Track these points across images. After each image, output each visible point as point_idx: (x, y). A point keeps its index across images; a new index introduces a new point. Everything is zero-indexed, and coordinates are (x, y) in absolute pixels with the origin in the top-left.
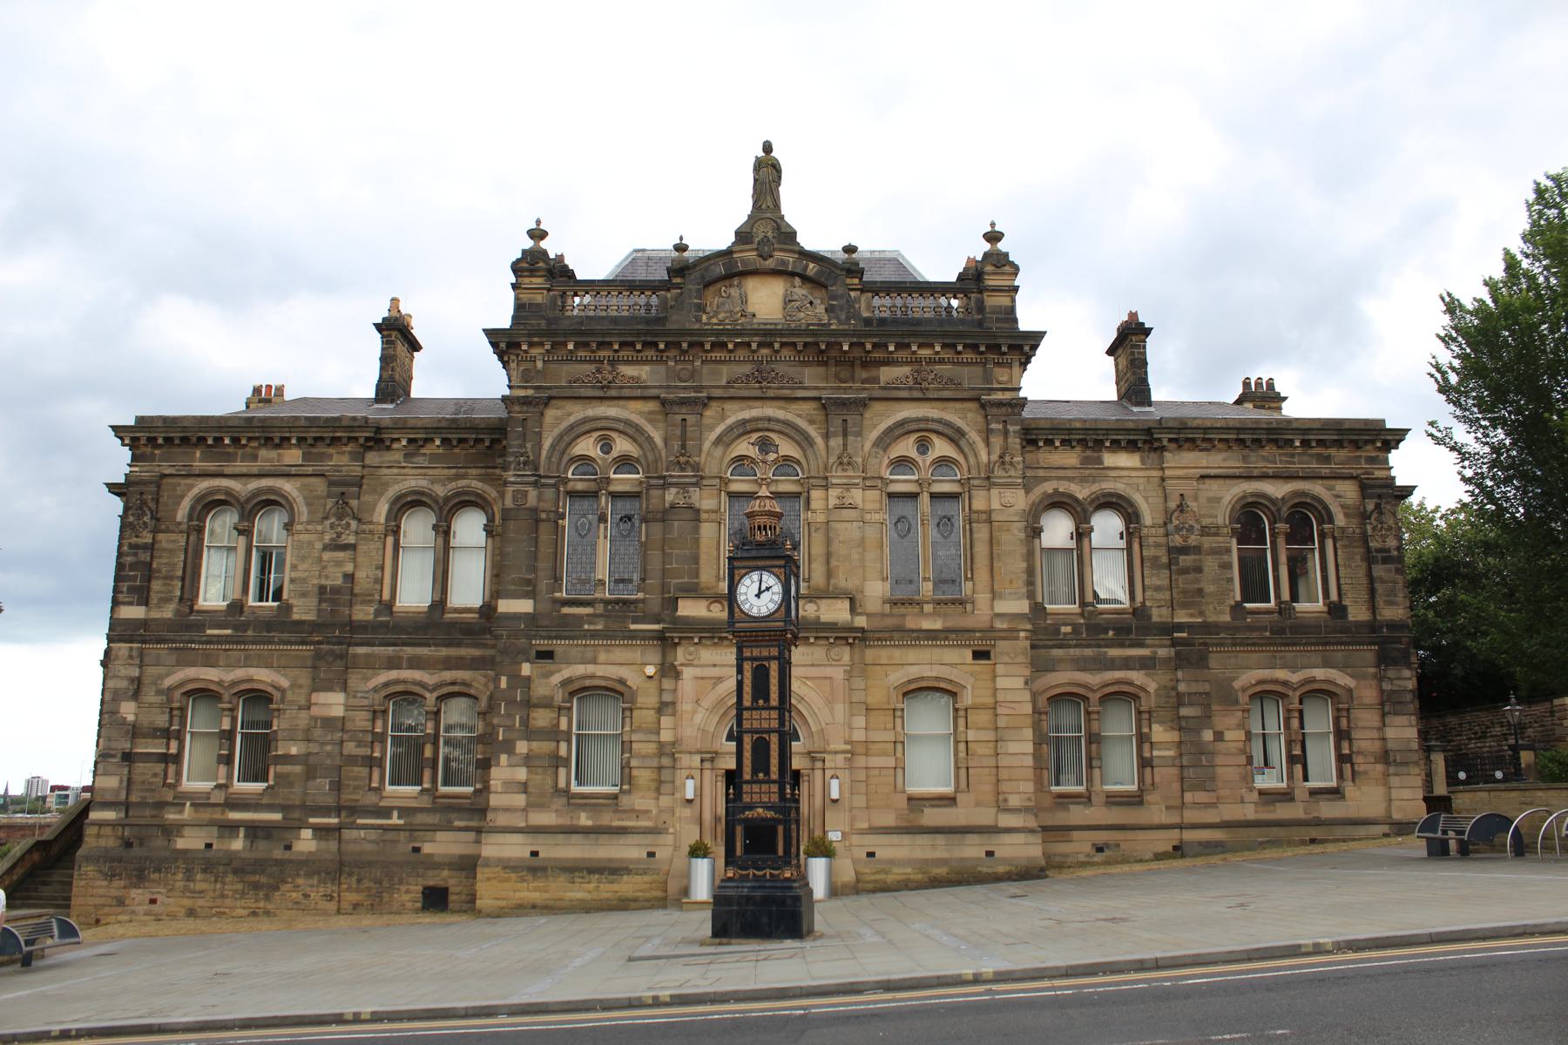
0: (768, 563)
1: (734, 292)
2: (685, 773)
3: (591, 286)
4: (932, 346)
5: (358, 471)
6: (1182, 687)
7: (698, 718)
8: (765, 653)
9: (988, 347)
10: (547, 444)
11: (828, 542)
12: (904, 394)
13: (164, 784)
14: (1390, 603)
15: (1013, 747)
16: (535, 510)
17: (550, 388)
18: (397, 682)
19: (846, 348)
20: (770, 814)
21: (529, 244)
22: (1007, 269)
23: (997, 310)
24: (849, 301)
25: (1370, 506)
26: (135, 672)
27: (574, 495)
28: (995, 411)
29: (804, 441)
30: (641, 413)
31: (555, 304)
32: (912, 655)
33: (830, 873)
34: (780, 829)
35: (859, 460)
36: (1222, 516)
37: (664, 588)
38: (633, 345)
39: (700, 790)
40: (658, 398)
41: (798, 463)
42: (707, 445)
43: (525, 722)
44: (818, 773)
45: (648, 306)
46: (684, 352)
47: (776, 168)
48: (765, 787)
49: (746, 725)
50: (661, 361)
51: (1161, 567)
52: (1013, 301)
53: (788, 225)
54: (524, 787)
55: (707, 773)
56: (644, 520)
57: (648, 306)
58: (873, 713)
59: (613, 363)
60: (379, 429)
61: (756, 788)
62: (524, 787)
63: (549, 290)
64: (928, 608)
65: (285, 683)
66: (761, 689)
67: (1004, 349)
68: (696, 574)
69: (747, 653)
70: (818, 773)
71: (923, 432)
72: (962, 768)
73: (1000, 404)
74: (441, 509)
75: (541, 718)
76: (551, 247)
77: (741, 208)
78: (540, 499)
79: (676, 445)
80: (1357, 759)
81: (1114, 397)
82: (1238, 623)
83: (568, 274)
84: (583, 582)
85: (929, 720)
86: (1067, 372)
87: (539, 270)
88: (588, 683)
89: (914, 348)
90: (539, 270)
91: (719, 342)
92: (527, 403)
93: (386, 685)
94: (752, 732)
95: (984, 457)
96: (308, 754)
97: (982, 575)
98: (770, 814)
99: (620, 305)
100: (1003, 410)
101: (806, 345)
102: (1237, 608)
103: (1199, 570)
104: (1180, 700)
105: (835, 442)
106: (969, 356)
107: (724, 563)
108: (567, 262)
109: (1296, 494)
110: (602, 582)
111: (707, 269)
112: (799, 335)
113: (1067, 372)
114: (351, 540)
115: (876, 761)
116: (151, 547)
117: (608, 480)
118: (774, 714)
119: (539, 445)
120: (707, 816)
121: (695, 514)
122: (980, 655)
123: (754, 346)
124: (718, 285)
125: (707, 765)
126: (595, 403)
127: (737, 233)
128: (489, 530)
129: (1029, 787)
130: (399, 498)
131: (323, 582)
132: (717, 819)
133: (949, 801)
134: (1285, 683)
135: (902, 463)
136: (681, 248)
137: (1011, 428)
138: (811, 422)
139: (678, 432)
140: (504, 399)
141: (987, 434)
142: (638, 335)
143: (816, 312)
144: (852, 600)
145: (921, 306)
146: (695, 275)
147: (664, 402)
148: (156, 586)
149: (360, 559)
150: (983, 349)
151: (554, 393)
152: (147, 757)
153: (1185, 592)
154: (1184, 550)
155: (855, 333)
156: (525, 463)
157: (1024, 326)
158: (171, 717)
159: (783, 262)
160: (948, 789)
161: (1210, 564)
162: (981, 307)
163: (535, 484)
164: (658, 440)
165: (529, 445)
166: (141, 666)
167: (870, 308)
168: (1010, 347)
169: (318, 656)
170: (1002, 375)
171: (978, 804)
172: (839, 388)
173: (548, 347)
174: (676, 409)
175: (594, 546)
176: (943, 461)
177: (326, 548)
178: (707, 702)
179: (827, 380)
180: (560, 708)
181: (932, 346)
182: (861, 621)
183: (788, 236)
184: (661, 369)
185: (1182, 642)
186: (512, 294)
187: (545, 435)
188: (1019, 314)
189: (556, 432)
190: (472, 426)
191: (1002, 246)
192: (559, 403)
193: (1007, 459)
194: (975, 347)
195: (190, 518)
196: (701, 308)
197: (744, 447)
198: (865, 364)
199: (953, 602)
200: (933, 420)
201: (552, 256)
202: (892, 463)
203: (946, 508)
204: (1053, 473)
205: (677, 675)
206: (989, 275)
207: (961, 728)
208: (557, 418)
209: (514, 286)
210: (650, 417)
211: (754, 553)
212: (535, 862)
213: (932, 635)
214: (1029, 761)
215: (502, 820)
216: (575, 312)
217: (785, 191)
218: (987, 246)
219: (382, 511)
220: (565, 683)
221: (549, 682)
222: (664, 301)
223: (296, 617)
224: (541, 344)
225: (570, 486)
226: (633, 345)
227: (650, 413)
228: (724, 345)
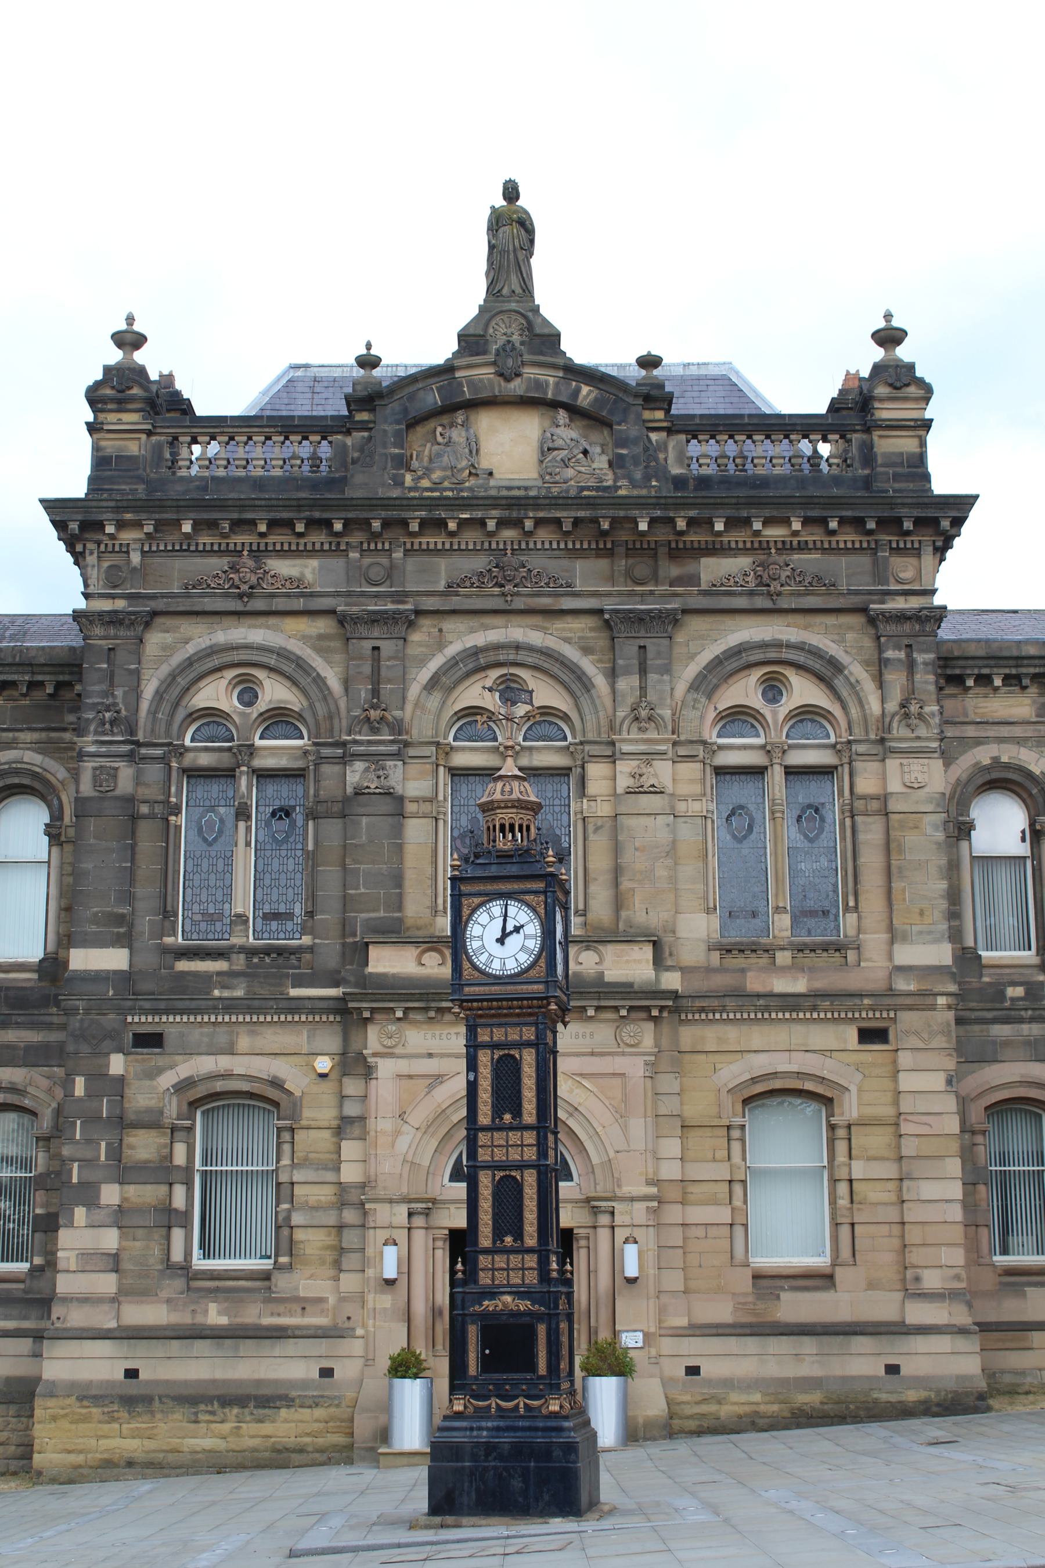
0: (516, 886)
1: (457, 435)
2: (382, 1235)
3: (219, 427)
4: (787, 522)
7: (403, 1144)
8: (514, 1035)
9: (881, 522)
10: (149, 690)
11: (617, 849)
12: (742, 602)
15: (929, 1190)
16: (130, 800)
17: (153, 597)
19: (643, 526)
20: (524, 1305)
21: (115, 356)
22: (912, 390)
23: (897, 460)
27: (194, 774)
28: (891, 629)
29: (575, 681)
30: (305, 638)
31: (160, 457)
32: (757, 1036)
33: (626, 1402)
34: (542, 1329)
35: (667, 713)
37: (345, 927)
38: (290, 524)
39: (407, 1264)
40: (332, 612)
41: (566, 718)
42: (414, 691)
43: (116, 1153)
44: (604, 1234)
45: (315, 460)
46: (375, 536)
47: (525, 225)
48: (515, 1260)
49: (483, 1155)
50: (337, 551)
52: (923, 444)
53: (546, 323)
54: (114, 1262)
55: (419, 1236)
56: (312, 815)
57: (315, 460)
58: (693, 1134)
59: (258, 554)
61: (500, 1261)
62: (114, 1262)
63: (149, 433)
64: (783, 958)
66: (507, 1096)
67: (908, 525)
68: (400, 907)
69: (484, 1036)
70: (604, 1234)
71: (773, 666)
72: (844, 1225)
73: (901, 617)
75: (143, 1146)
76: (152, 360)
77: (466, 294)
78: (138, 781)
79: (363, 691)
83: (181, 406)
84: (211, 918)
85: (786, 1144)
87: (132, 399)
88: (219, 1086)
89: (757, 525)
90: (132, 399)
91: (436, 518)
92: (115, 623)
95: (874, 706)
97: (873, 901)
98: (524, 1305)
99: (268, 458)
100: (907, 627)
101: (577, 522)
105: (628, 684)
106: (849, 537)
107: (444, 888)
108: (178, 386)
110: (242, 919)
111: (411, 397)
112: (565, 506)
115: (698, 1214)
117: (251, 750)
118: (530, 1138)
120: (420, 1308)
121: (396, 806)
122: (870, 1035)
123: (491, 525)
124: (431, 424)
125: (419, 1221)
126: (227, 621)
127: (462, 337)
128: (54, 834)
129: (957, 1257)
132: (435, 1312)
133: (822, 1280)
135: (738, 717)
136: (369, 362)
137: (920, 658)
138: (587, 650)
139: (367, 669)
140: (77, 615)
141: (879, 667)
142: (299, 508)
143: (594, 467)
144: (656, 945)
145: (767, 456)
146: (393, 407)
147: (342, 620)
150: (871, 525)
151: (160, 605)
155: (658, 502)
156: (113, 722)
157: (942, 485)
159: (539, 385)
160: (821, 1261)
162: (868, 456)
163: (131, 757)
164: (334, 683)
165: (119, 692)
167: (683, 459)
168: (918, 522)
170: (904, 568)
171: (872, 1285)
172: (631, 594)
173: (149, 529)
174: (362, 630)
175: (228, 860)
176: (806, 715)
178: (418, 1116)
179: (612, 579)
180: (173, 1129)
181: (787, 522)
182: (672, 981)
183: (547, 341)
184: (337, 564)
186: (86, 442)
187: (146, 674)
188: (934, 465)
189: (165, 670)
190: (25, 662)
191: (904, 352)
193: (914, 708)
194: (858, 523)
196: (403, 463)
197: (476, 693)
198: (678, 553)
199: (825, 948)
200: (789, 646)
201: (154, 376)
202: (721, 717)
203: (812, 791)
204: (992, 732)
205: (368, 1072)
206: (882, 402)
207: (841, 1157)
208: (165, 648)
209: (92, 428)
210: (319, 643)
211: (494, 871)
212: (132, 1388)
213: (790, 1003)
214: (956, 1213)
215: (77, 1317)
216: (194, 470)
217: (540, 264)
218: (878, 354)
220: (182, 1087)
222: (341, 452)
224: (138, 525)
225: (188, 760)
226: (290, 524)
227: (321, 637)
228: (442, 523)
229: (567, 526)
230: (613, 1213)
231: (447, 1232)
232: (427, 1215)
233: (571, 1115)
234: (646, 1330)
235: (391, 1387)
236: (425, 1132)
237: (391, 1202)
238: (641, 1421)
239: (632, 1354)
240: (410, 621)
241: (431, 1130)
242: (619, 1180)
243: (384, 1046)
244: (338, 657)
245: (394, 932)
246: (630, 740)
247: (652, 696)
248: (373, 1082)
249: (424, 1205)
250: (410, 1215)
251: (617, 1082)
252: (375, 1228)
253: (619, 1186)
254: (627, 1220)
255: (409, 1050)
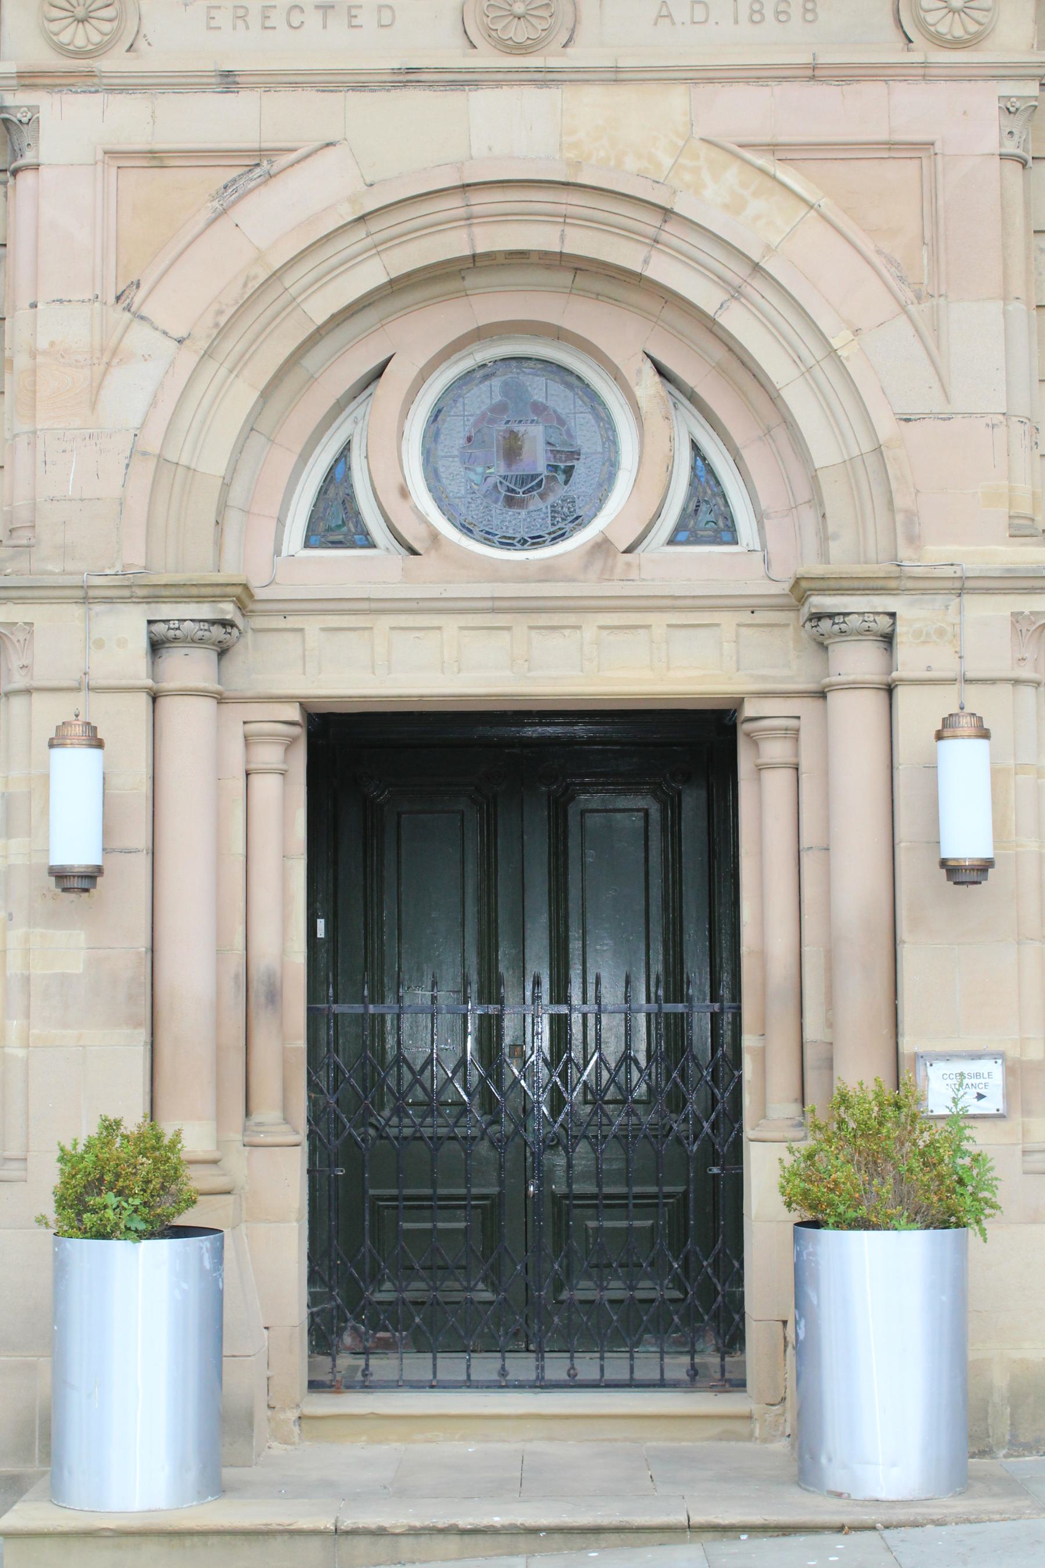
2: (48, 712)
7: (132, 395)
39: (143, 819)
44: (855, 715)
55: (189, 721)
58: (883, 695)
70: (855, 715)
120: (193, 976)
125: (190, 668)
132: (254, 993)
178: (187, 297)
230: (888, 639)
231: (294, 713)
232: (223, 652)
233: (736, 293)
234: (1013, 1053)
235: (60, 1268)
236: (208, 354)
237: (86, 600)
238: (1000, 1380)
239: (981, 1139)
241: (233, 346)
242: (911, 516)
243: (62, 50)
248: (26, 179)
249: (205, 611)
250: (156, 646)
251: (903, 173)
252: (28, 691)
253: (913, 539)
254: (945, 664)
255: (153, 60)
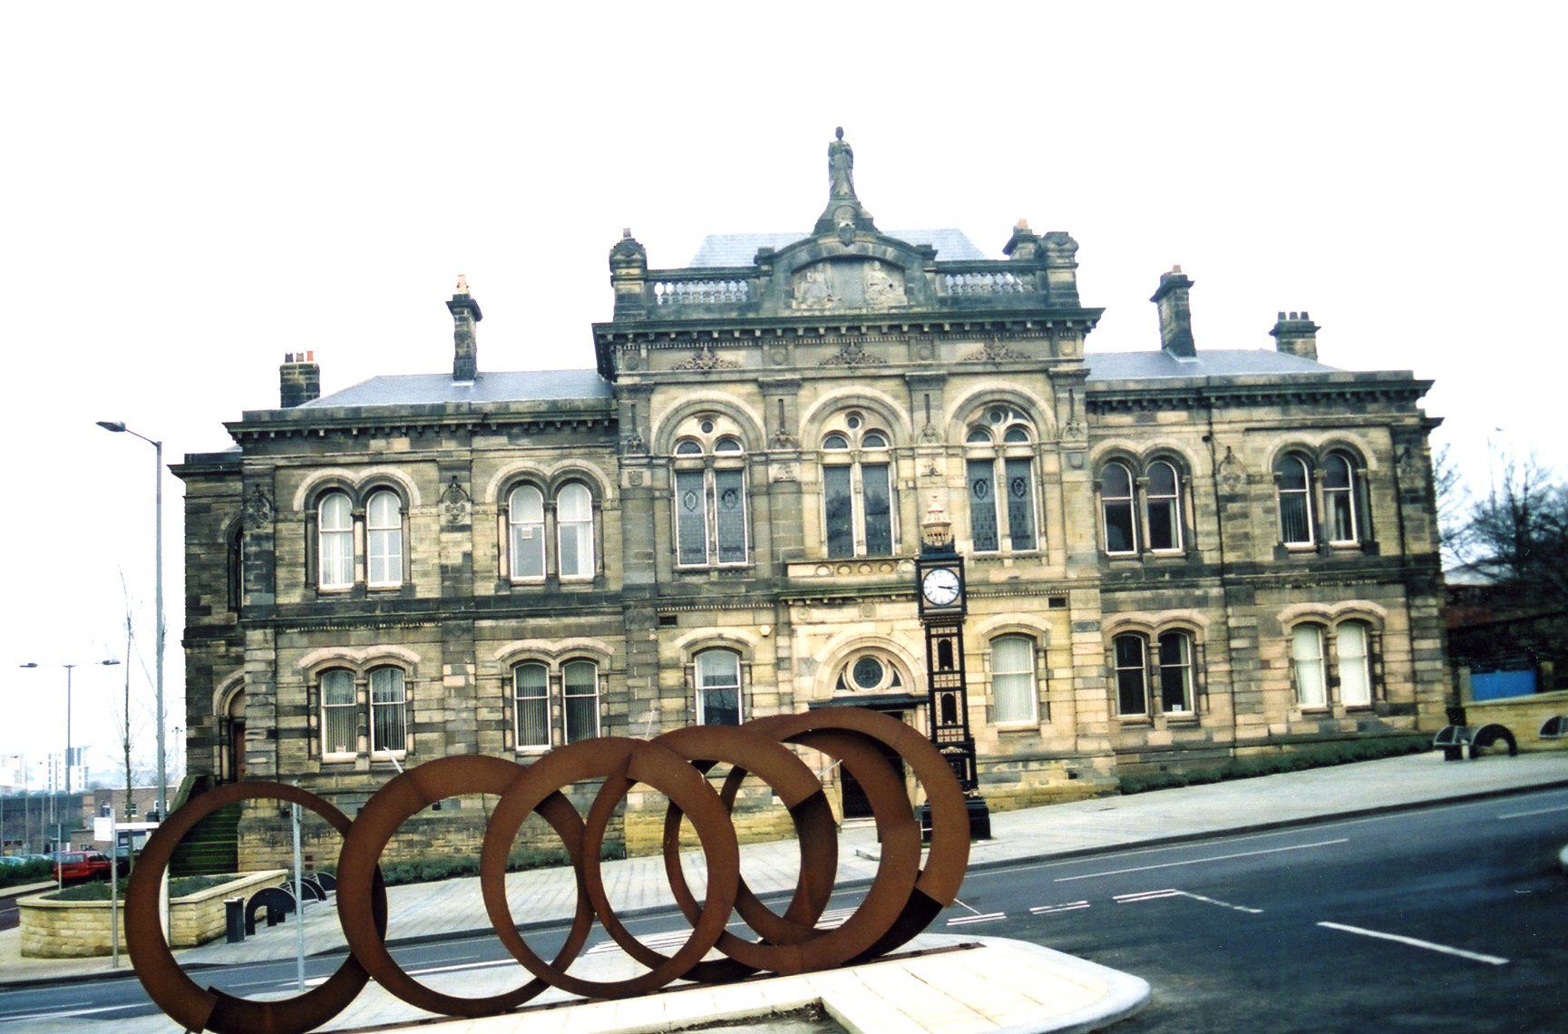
5: (467, 456)
6: (1232, 622)
8: (947, 631)
10: (655, 426)
13: (310, 757)
14: (1417, 539)
16: (650, 489)
18: (523, 651)
20: (959, 751)
24: (926, 283)
25: (1400, 450)
26: (272, 655)
27: (681, 473)
28: (1062, 382)
30: (740, 395)
36: (1265, 465)
37: (773, 555)
40: (755, 381)
41: (883, 432)
48: (954, 731)
51: (1209, 514)
60: (486, 416)
61: (947, 732)
65: (415, 657)
66: (946, 658)
68: (802, 541)
69: (933, 631)
73: (1067, 375)
74: (549, 488)
79: (775, 425)
80: (1389, 679)
81: (1158, 347)
82: (1282, 563)
86: (1122, 340)
93: (513, 654)
94: (941, 690)
96: (445, 722)
97: (1055, 531)
98: (959, 751)
102: (1280, 549)
103: (1245, 515)
104: (1230, 634)
109: (1333, 442)
111: (793, 257)
113: (1122, 340)
114: (467, 521)
116: (272, 537)
118: (958, 676)
119: (649, 429)
121: (798, 487)
129: (1103, 717)
130: (508, 479)
131: (444, 562)
134: (1324, 615)
138: (896, 397)
139: (776, 412)
141: (1056, 402)
146: (784, 263)
147: (762, 385)
148: (282, 573)
149: (477, 539)
151: (658, 379)
152: (291, 732)
153: (1233, 536)
154: (1232, 498)
156: (639, 446)
158: (309, 694)
161: (1256, 510)
162: (1045, 283)
163: (650, 466)
164: (759, 421)
165: (640, 430)
166: (276, 649)
169: (446, 631)
170: (1066, 347)
174: (773, 391)
177: (442, 530)
183: (864, 224)
184: (757, 354)
185: (1232, 582)
188: (1080, 289)
189: (663, 416)
192: (663, 388)
193: (1074, 425)
195: (306, 506)
196: (791, 295)
197: (839, 422)
199: (1030, 557)
204: (1112, 432)
205: (792, 633)
208: (663, 404)
219: (491, 492)
220: (688, 646)
221: (673, 645)
223: (419, 595)
227: (749, 394)
229: (885, 330)
240: (796, 385)
244: (761, 406)
245: (801, 557)
246: (924, 446)
247: (932, 421)
